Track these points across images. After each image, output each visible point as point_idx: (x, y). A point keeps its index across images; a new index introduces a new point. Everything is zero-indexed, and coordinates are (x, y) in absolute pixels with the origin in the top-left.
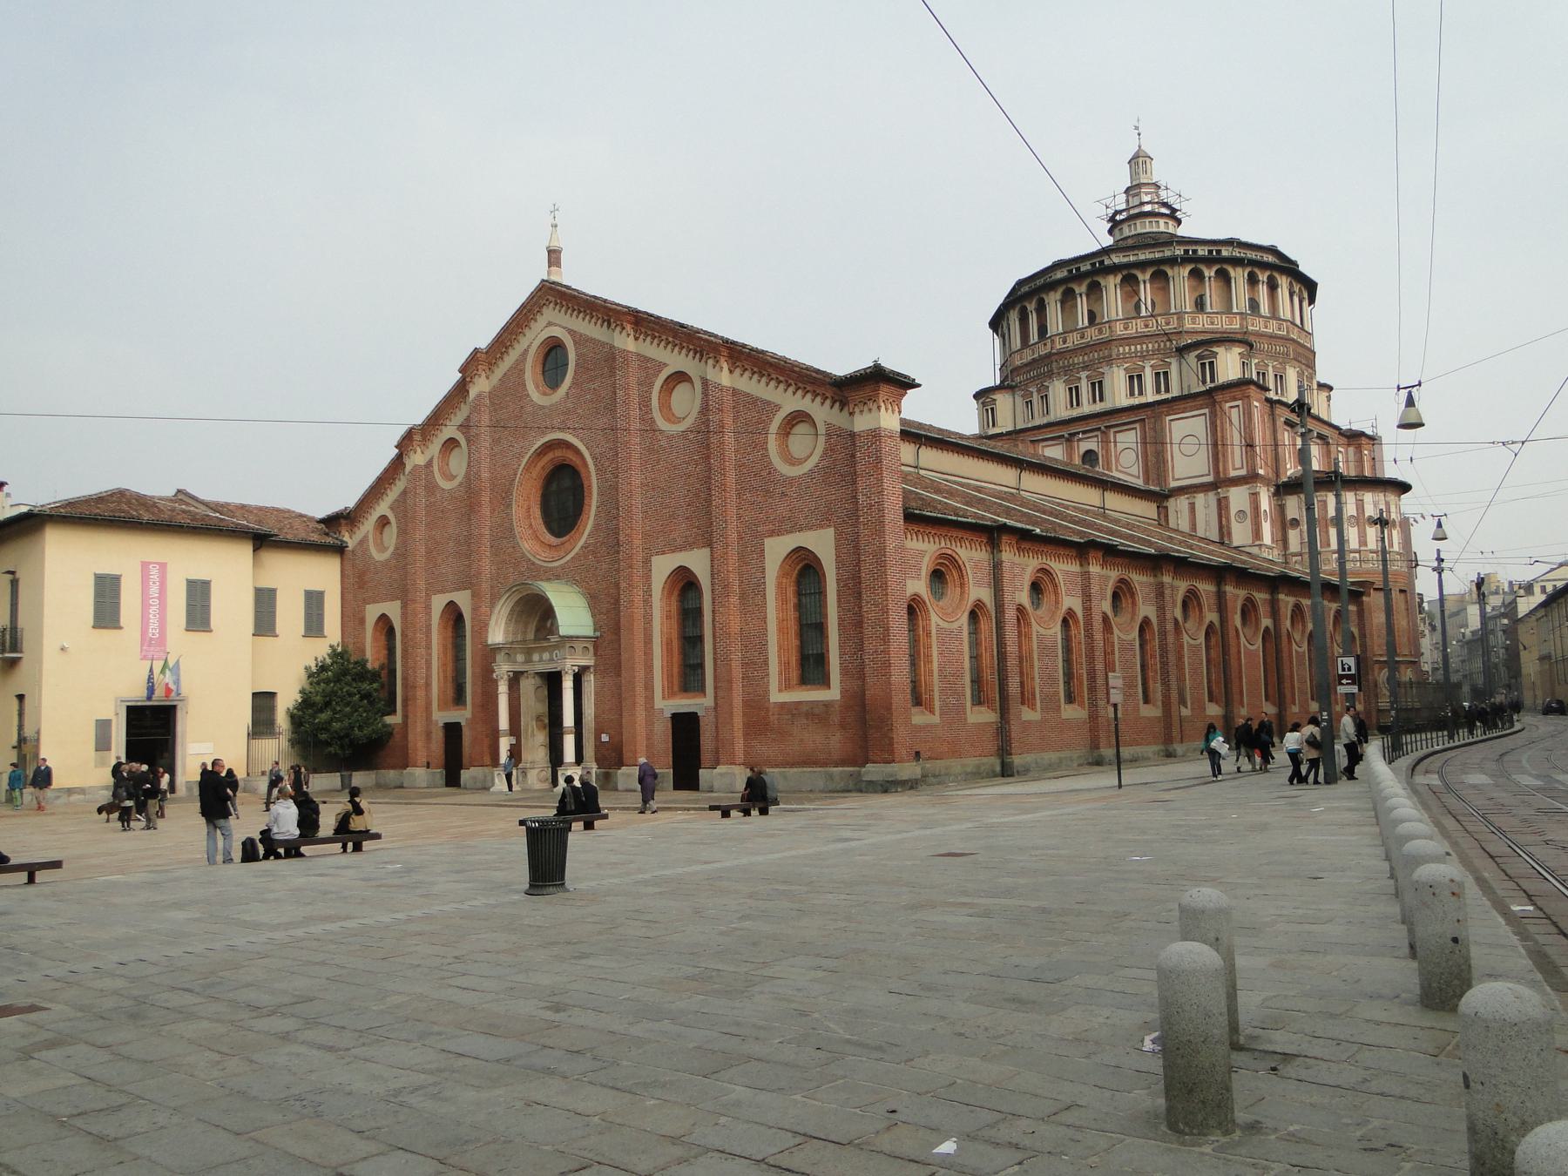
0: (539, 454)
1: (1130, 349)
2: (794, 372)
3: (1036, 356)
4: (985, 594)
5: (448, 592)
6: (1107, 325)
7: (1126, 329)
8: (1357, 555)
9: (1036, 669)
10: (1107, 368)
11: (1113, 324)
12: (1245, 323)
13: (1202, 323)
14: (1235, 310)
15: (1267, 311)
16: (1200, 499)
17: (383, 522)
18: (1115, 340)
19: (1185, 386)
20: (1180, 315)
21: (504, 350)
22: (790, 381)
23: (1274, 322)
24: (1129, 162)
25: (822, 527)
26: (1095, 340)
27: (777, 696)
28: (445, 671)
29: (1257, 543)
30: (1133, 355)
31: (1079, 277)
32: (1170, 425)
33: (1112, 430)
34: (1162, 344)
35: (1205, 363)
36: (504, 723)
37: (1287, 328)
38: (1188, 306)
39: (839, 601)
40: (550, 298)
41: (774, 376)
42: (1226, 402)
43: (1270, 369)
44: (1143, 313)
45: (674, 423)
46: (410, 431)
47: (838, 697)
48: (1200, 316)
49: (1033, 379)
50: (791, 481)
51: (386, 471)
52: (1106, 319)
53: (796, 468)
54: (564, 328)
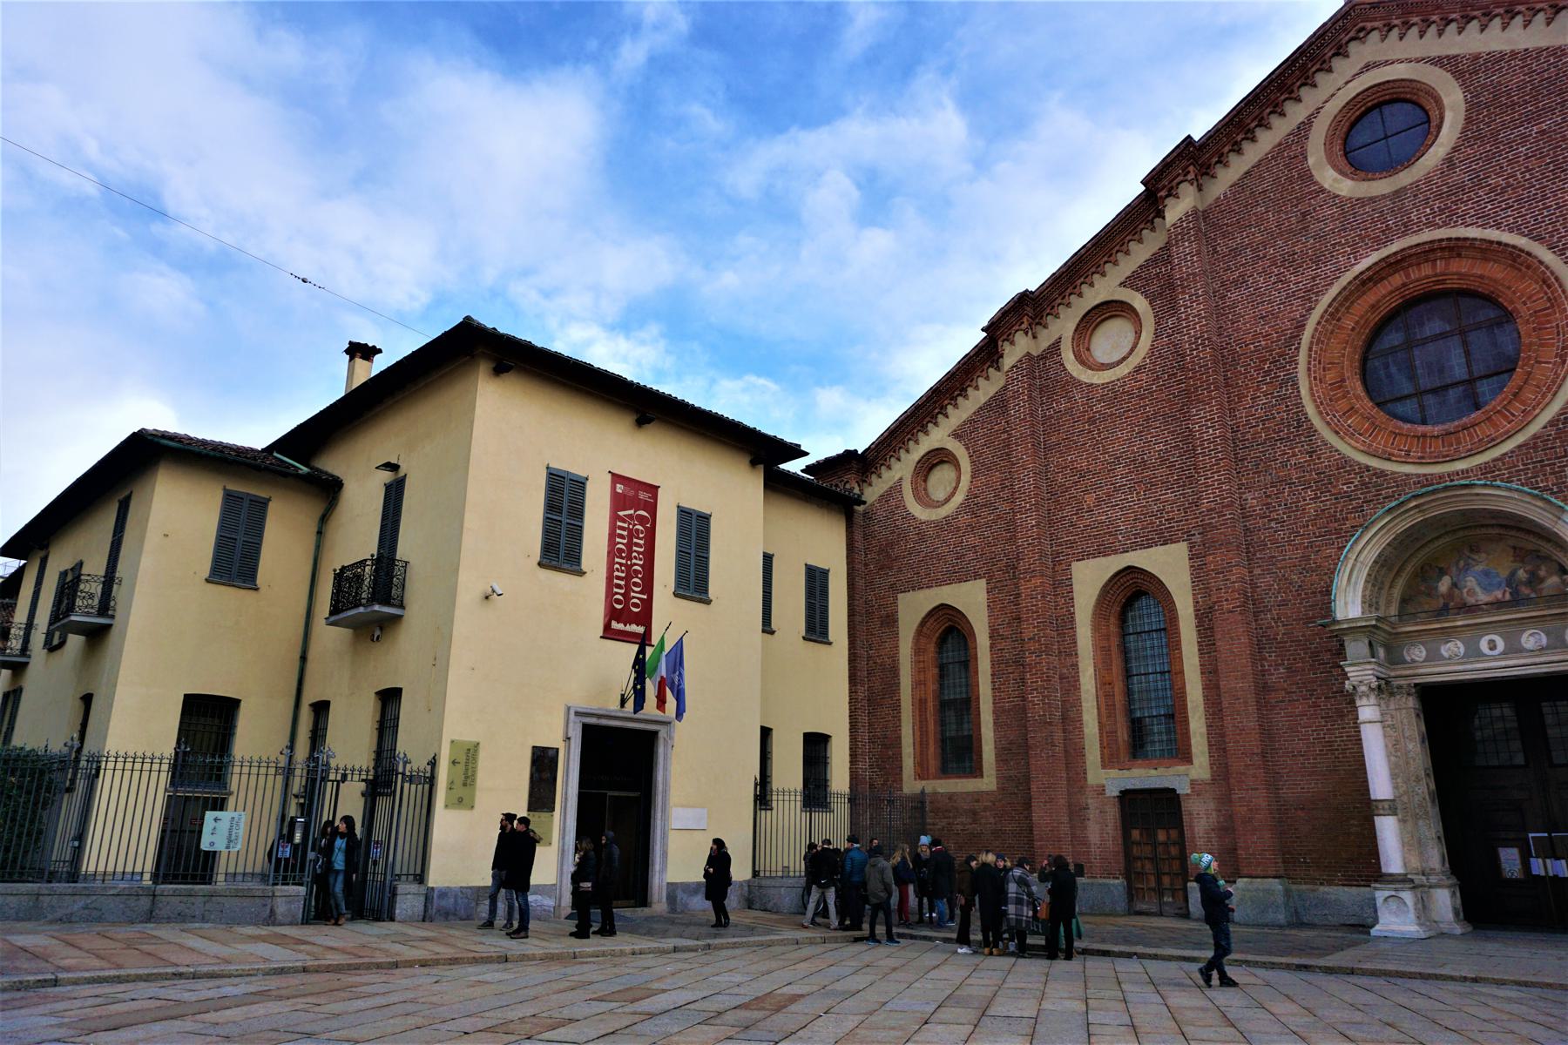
0: (1364, 283)
5: (1115, 552)
17: (938, 458)
28: (1109, 696)
51: (950, 377)
54: (1418, 61)
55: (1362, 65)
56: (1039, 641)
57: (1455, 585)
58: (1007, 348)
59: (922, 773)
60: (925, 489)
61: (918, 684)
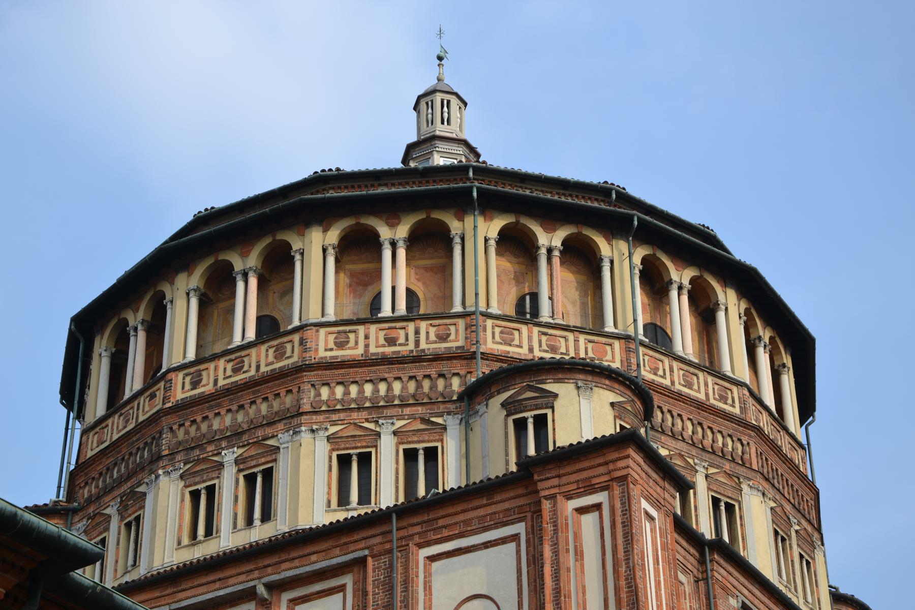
1: (347, 393)
6: (296, 338)
7: (340, 345)
10: (284, 437)
11: (310, 333)
12: (633, 361)
14: (609, 328)
18: (310, 367)
23: (710, 379)
32: (428, 575)
33: (286, 596)
34: (426, 384)
35: (525, 420)
37: (743, 402)
42: (569, 497)
48: (524, 329)
52: (296, 323)
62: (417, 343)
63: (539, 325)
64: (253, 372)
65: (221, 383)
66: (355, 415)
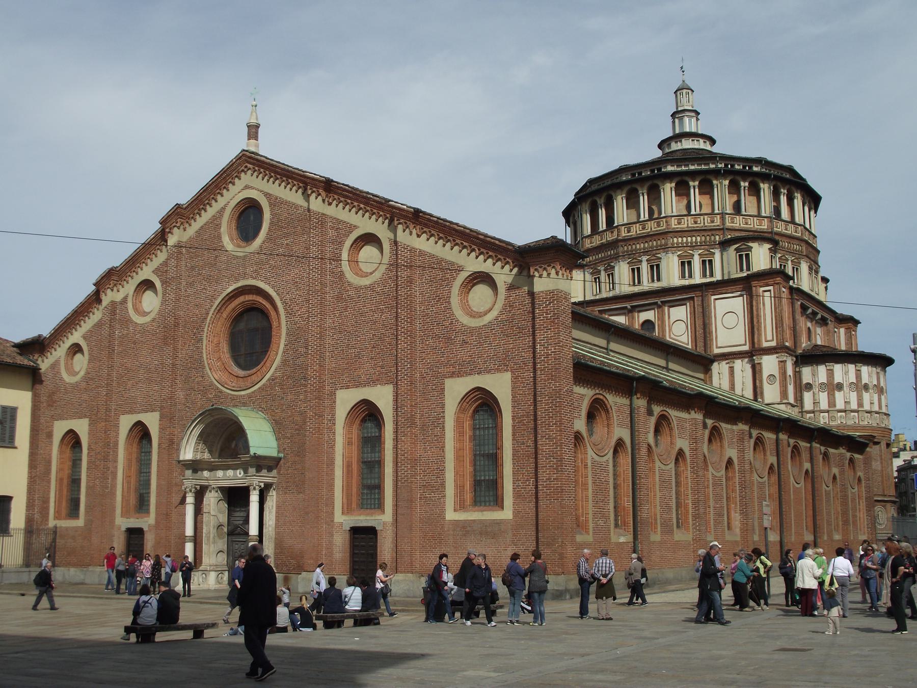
0: (230, 298)
1: (682, 240)
2: (478, 239)
3: (604, 241)
4: (626, 435)
6: (664, 220)
7: (679, 223)
8: (856, 414)
9: (658, 499)
10: (664, 254)
11: (669, 219)
13: (739, 222)
15: (787, 217)
16: (738, 364)
17: (76, 349)
19: (726, 272)
20: (723, 215)
21: (202, 206)
22: (474, 247)
23: (793, 226)
24: (675, 92)
25: (498, 370)
26: (653, 231)
27: (451, 515)
28: (129, 483)
29: (784, 401)
30: (685, 245)
31: (642, 180)
33: (667, 305)
34: (708, 238)
36: (189, 531)
38: (727, 209)
39: (514, 435)
40: (250, 166)
41: (458, 241)
43: (789, 262)
44: (693, 212)
45: (362, 277)
46: (109, 271)
47: (511, 517)
48: (737, 217)
49: (601, 261)
50: (472, 331)
52: (663, 215)
53: (477, 320)
55: (244, 185)
56: (101, 454)
57: (236, 445)
58: (103, 297)
59: (57, 517)
60: (72, 364)
61: (60, 470)
62: (704, 223)
63: (742, 215)
64: (649, 230)
65: (638, 232)
66: (686, 248)
